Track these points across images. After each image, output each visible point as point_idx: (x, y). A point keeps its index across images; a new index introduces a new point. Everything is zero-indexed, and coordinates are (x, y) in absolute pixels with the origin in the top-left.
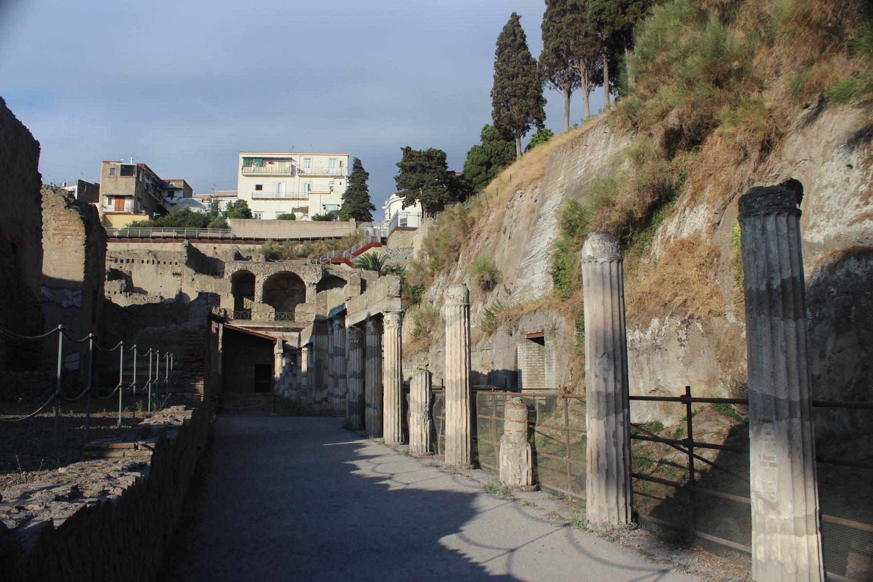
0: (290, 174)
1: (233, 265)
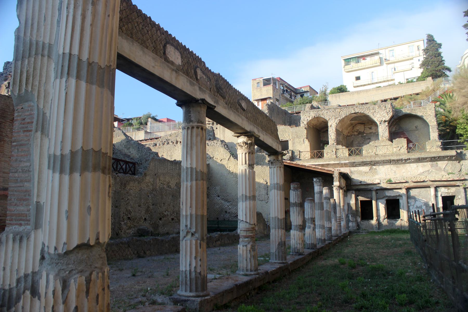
0: (379, 64)
1: (307, 114)
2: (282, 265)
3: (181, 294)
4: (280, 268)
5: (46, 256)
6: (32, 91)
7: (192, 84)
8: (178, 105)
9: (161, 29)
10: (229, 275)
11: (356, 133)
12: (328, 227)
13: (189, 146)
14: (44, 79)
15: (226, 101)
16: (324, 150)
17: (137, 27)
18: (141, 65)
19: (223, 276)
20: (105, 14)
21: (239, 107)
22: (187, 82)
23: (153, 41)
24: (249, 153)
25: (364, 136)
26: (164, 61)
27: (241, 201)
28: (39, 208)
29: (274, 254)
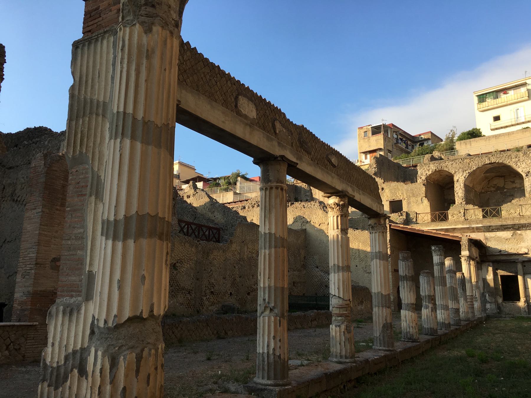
0: (527, 98)
1: (426, 168)
2: (388, 353)
3: (257, 382)
4: (385, 356)
5: (96, 330)
6: (86, 153)
7: (269, 139)
8: (255, 162)
9: (232, 78)
10: (320, 362)
11: (493, 189)
12: (455, 309)
13: (268, 208)
14: (99, 139)
15: (312, 156)
16: (449, 211)
17: (204, 78)
18: (208, 120)
19: (312, 363)
20: (161, 68)
21: (328, 162)
22: (264, 137)
23: (223, 93)
24: (341, 216)
25: (505, 192)
26: (236, 114)
27: (333, 272)
28: (91, 277)
29: (378, 339)
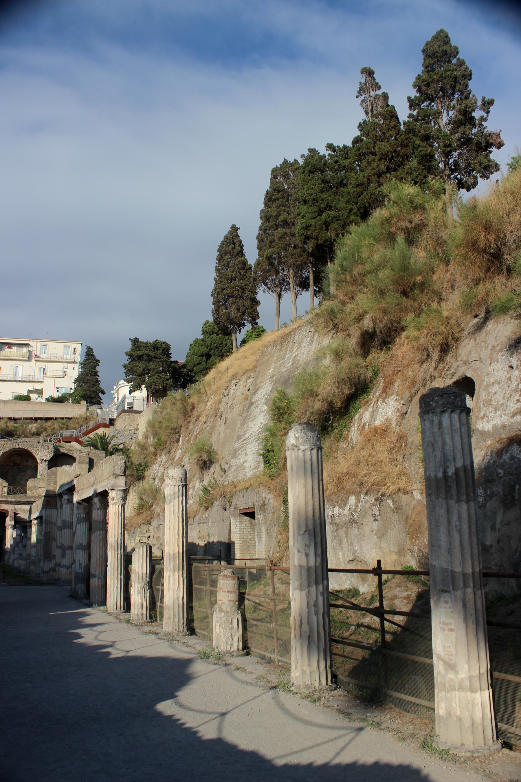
0: (27, 359)
